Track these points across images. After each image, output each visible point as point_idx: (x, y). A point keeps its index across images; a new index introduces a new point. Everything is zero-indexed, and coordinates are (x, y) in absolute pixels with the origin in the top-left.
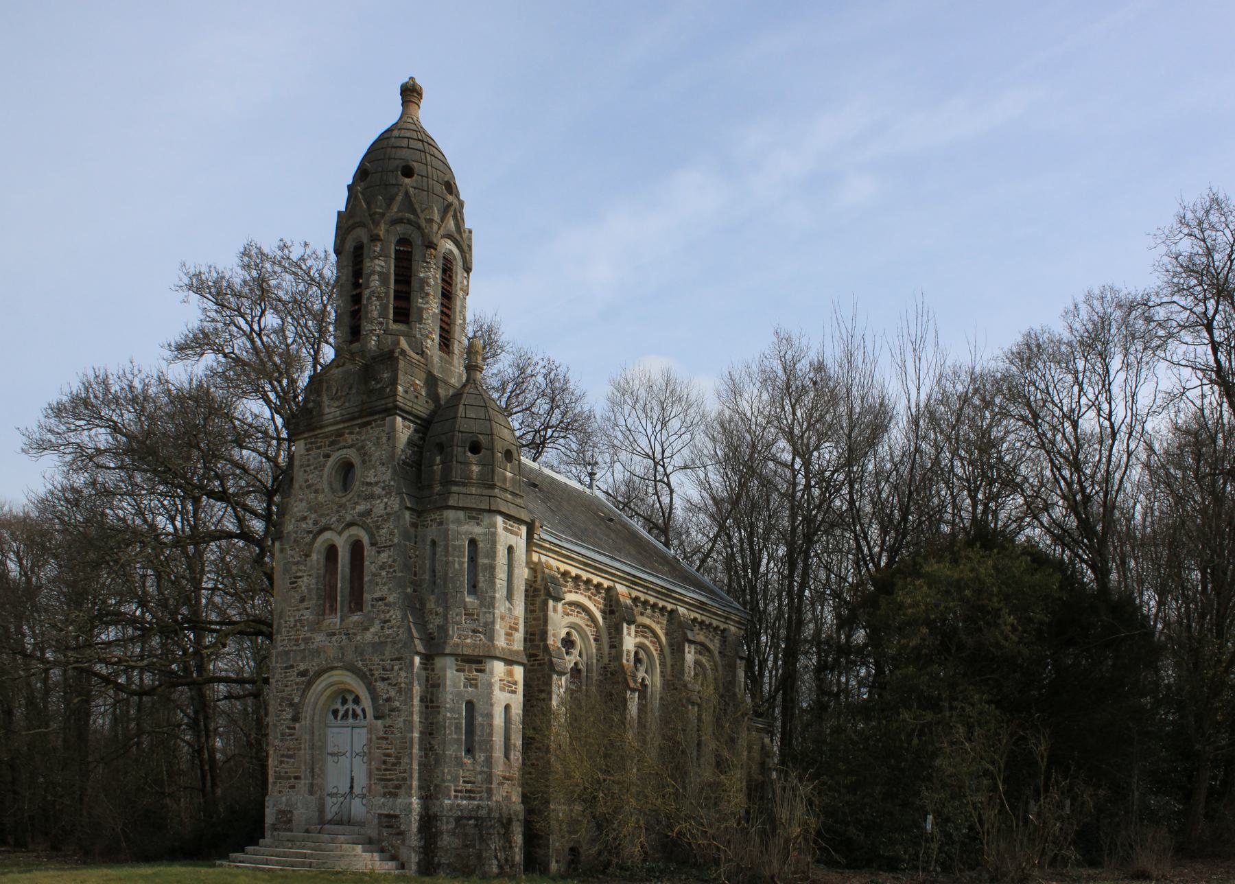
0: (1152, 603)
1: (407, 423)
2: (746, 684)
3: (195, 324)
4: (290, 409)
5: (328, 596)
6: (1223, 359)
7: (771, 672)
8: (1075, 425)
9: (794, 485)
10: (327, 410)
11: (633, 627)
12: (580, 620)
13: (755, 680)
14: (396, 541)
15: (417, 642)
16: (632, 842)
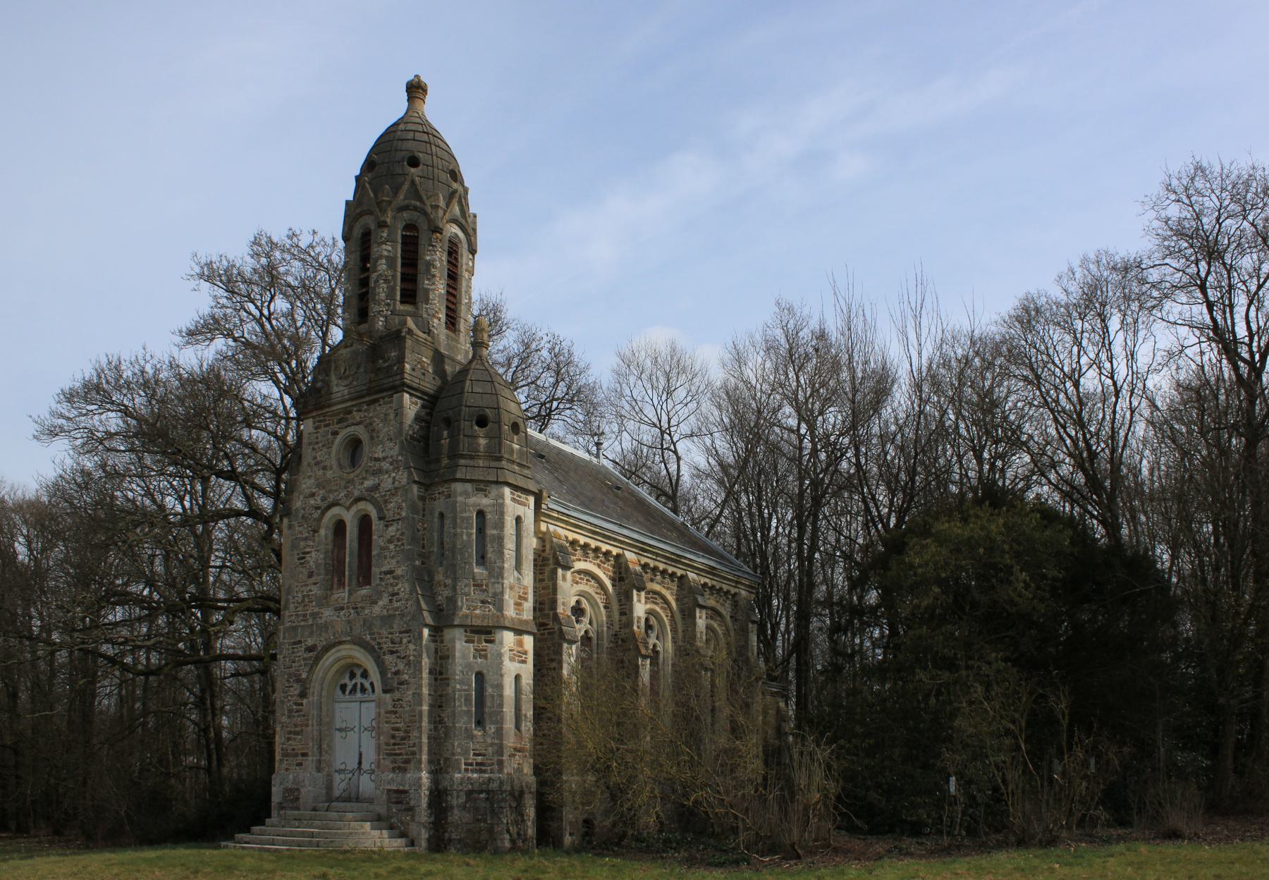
0: (1165, 557)
1: (414, 399)
2: (759, 648)
3: (206, 310)
4: (299, 389)
5: (336, 569)
6: (1219, 318)
7: (783, 636)
8: (1076, 385)
9: (801, 449)
10: (335, 389)
11: (643, 594)
12: (590, 588)
13: (767, 643)
14: (404, 514)
15: (426, 614)
16: (647, 812)
